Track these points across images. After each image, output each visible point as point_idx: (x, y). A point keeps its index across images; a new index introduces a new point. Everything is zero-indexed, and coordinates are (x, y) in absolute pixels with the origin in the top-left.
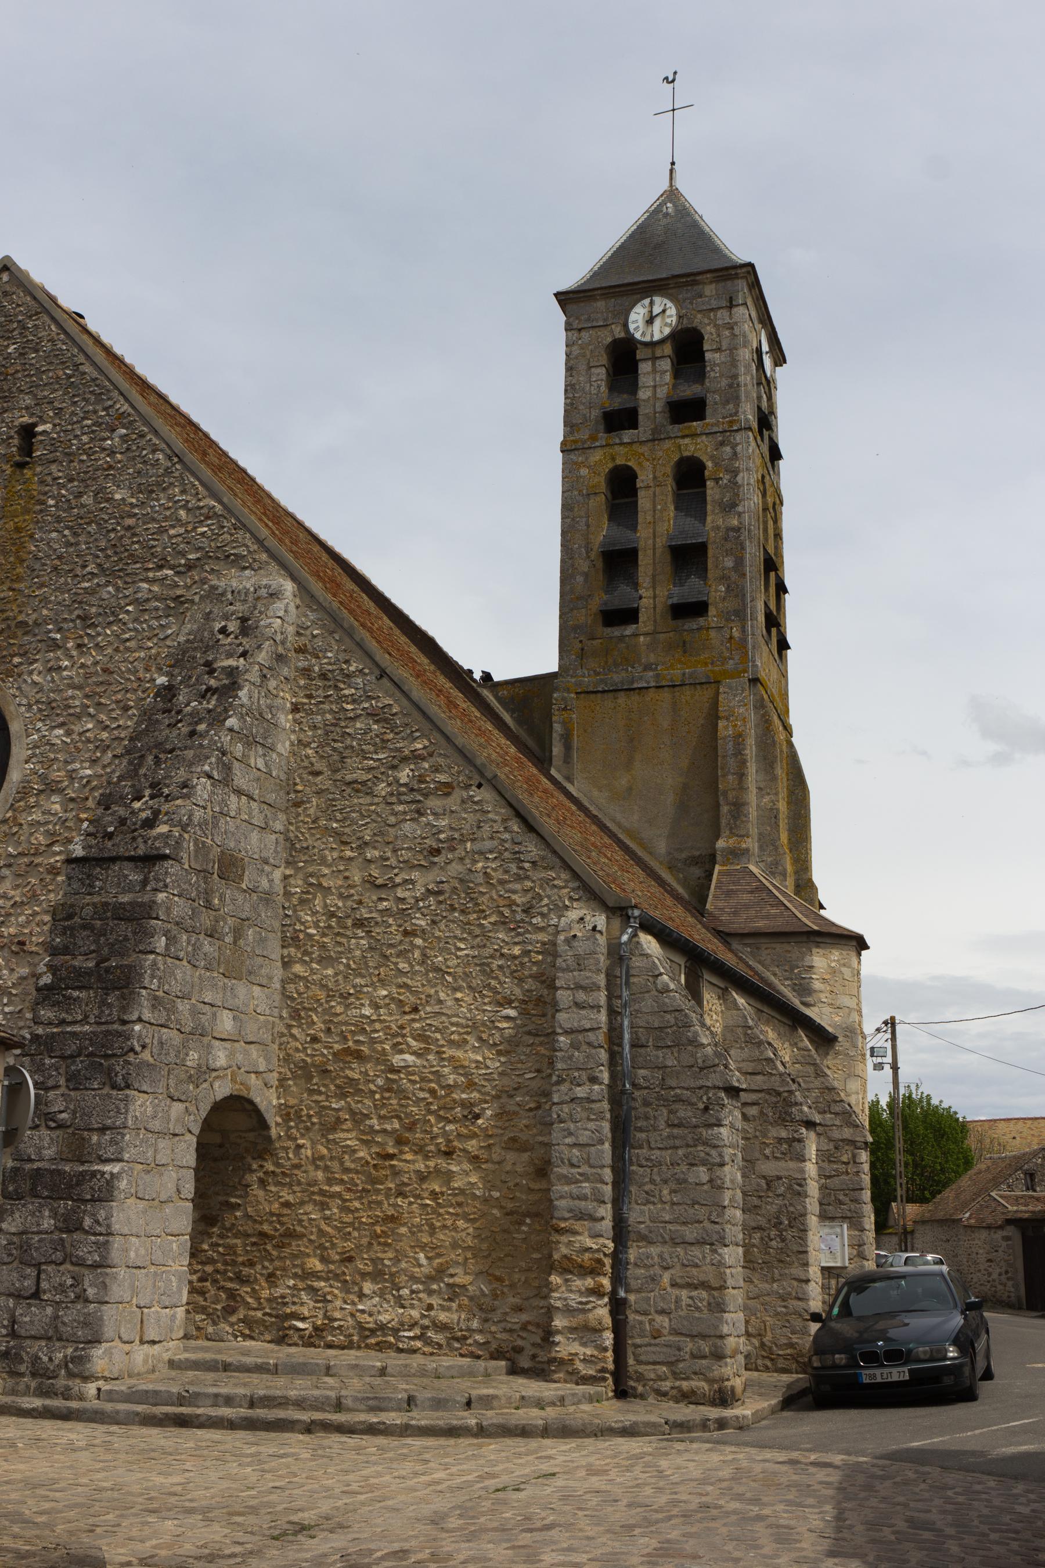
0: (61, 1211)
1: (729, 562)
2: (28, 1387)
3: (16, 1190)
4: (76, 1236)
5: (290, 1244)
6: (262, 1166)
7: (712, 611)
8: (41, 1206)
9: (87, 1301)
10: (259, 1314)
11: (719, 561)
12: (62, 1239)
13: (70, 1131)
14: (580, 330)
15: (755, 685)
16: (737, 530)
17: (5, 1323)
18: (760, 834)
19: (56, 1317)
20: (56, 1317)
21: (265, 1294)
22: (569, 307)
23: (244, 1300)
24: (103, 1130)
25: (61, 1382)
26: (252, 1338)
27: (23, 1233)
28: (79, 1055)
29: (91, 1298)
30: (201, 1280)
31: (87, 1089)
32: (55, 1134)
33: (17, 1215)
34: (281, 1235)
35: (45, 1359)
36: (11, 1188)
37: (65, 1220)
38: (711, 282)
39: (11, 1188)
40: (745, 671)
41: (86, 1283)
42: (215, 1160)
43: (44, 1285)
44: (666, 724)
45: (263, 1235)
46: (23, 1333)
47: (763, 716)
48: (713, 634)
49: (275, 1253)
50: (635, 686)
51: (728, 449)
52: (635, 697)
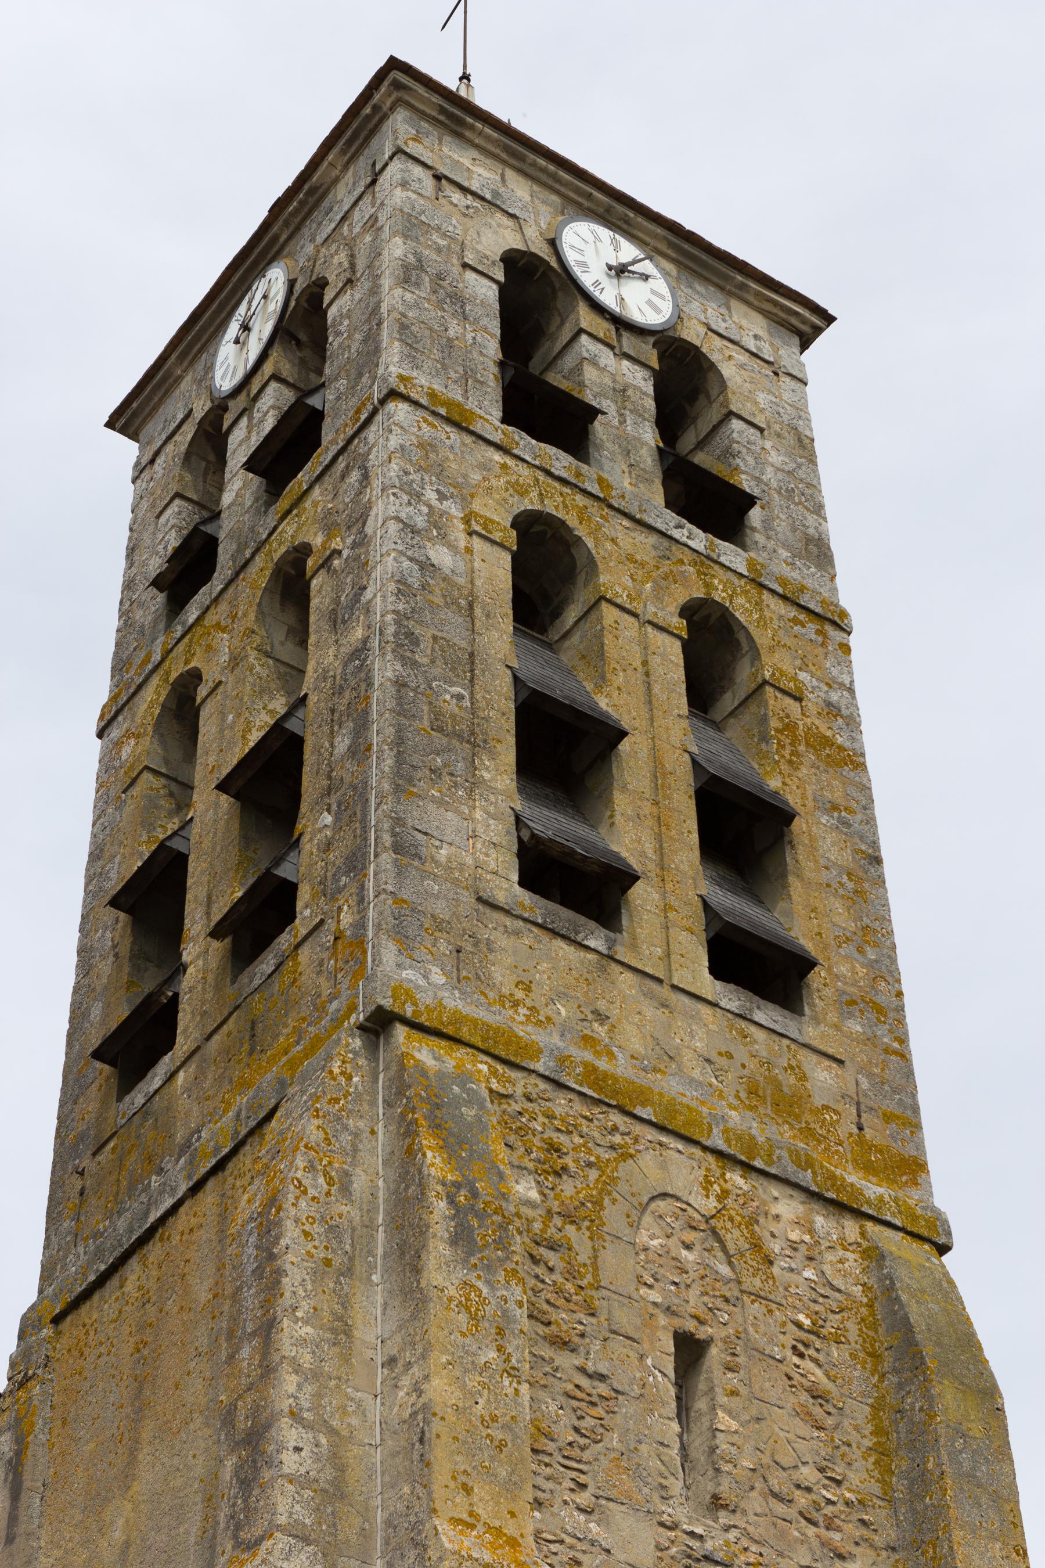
7: (304, 894)
14: (152, 461)
15: (389, 1036)
16: (361, 651)
18: (388, 1523)
22: (141, 437)
38: (346, 167)
40: (352, 1008)
44: (202, 1293)
47: (403, 1116)
48: (305, 955)
50: (152, 1218)
51: (355, 476)
52: (155, 1251)
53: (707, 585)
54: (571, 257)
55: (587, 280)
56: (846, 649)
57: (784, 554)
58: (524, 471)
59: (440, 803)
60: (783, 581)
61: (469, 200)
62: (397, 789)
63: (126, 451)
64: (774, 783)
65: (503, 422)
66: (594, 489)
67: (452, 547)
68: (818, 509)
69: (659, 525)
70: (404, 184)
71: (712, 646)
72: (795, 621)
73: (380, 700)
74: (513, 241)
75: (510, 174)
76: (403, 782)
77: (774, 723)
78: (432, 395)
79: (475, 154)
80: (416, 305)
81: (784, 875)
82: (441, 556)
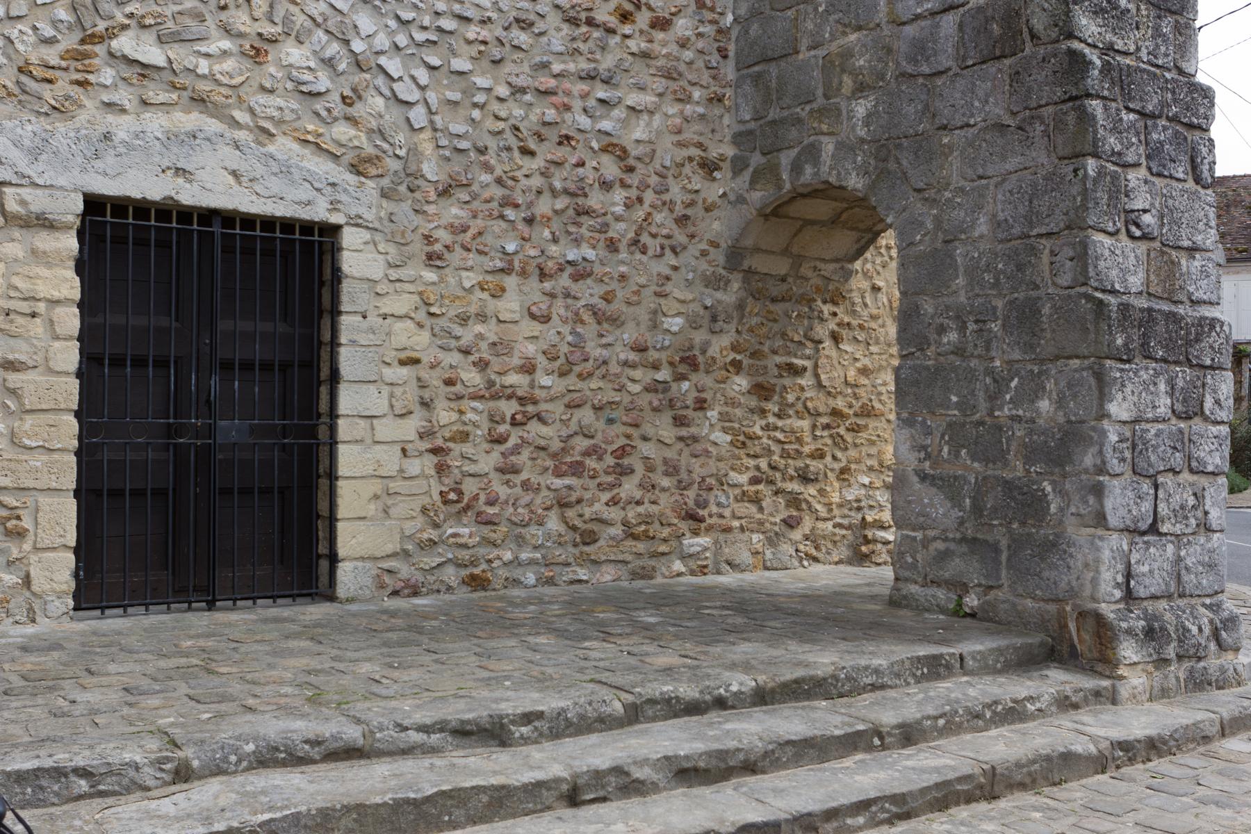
0: (1180, 383)
2: (1177, 679)
3: (1126, 345)
4: (1197, 424)
5: (866, 426)
6: (835, 314)
8: (1157, 374)
9: (1209, 530)
10: (829, 525)
12: (1181, 431)
13: (1157, 244)
17: (1120, 579)
19: (1179, 559)
20: (1179, 559)
21: (836, 498)
23: (810, 507)
24: (1193, 250)
25: (1214, 662)
26: (816, 560)
27: (1136, 421)
28: (1160, 117)
29: (1214, 527)
30: (755, 481)
31: (1171, 177)
32: (1143, 247)
33: (1128, 390)
34: (856, 415)
35: (1195, 630)
36: (1119, 342)
37: (1185, 400)
39: (1119, 342)
41: (1208, 502)
42: (774, 300)
43: (1163, 509)
45: (835, 413)
46: (1142, 592)
49: (849, 437)
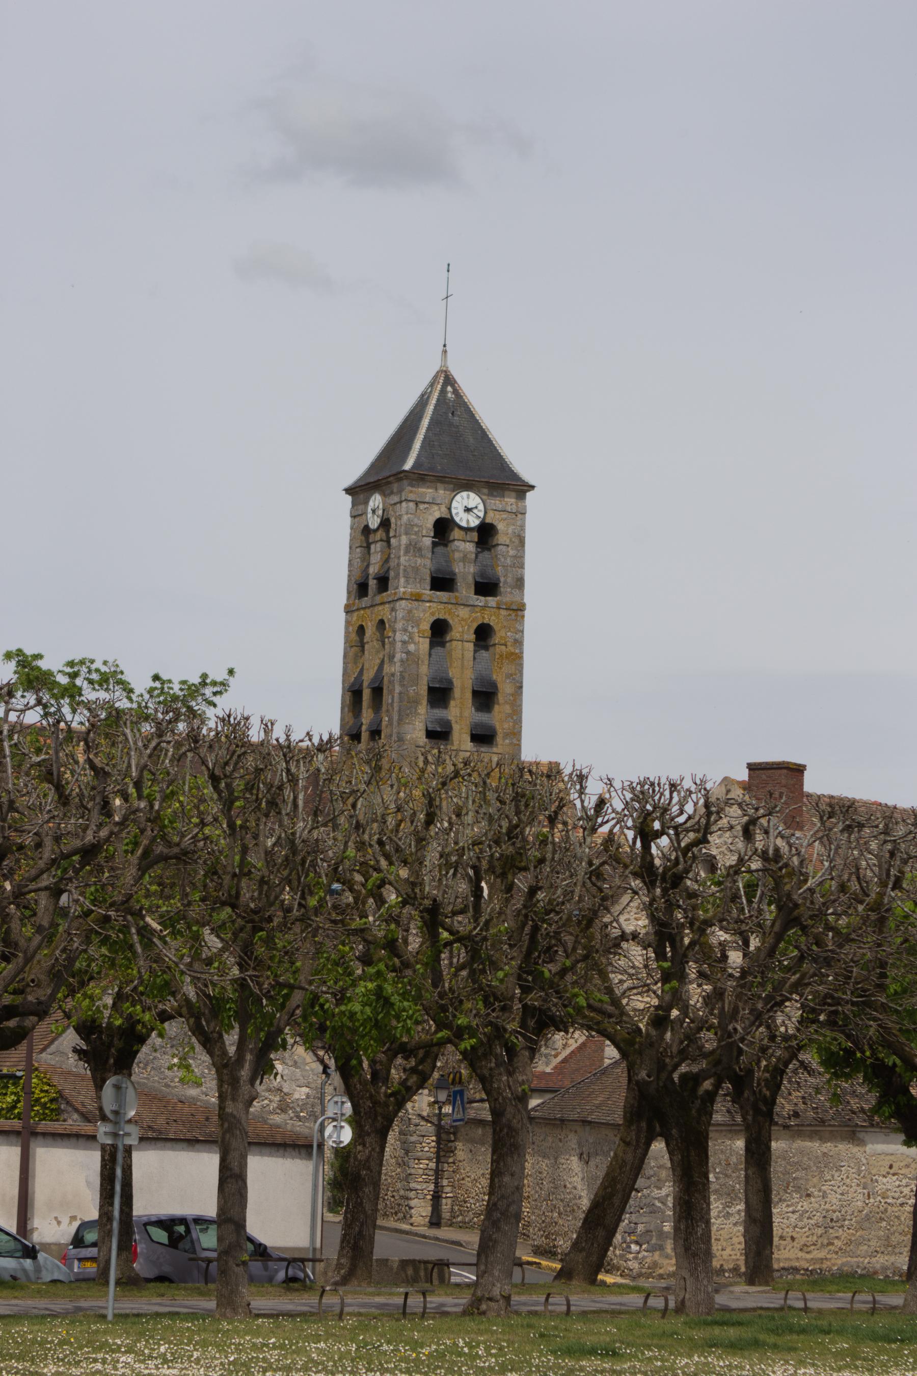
1: (390, 701)
11: (387, 698)
53: (483, 618)
54: (454, 512)
55: (457, 519)
56: (523, 617)
57: (509, 590)
58: (435, 605)
59: (409, 723)
60: (506, 604)
61: (426, 506)
62: (399, 724)
63: (349, 498)
64: (494, 677)
65: (431, 590)
66: (453, 601)
67: (415, 643)
68: (522, 566)
69: (472, 603)
70: (407, 514)
71: (483, 634)
72: (510, 615)
73: (396, 696)
74: (437, 515)
75: (439, 485)
76: (400, 720)
77: (497, 656)
78: (411, 594)
79: (428, 484)
80: (409, 560)
81: (494, 703)
82: (412, 647)
